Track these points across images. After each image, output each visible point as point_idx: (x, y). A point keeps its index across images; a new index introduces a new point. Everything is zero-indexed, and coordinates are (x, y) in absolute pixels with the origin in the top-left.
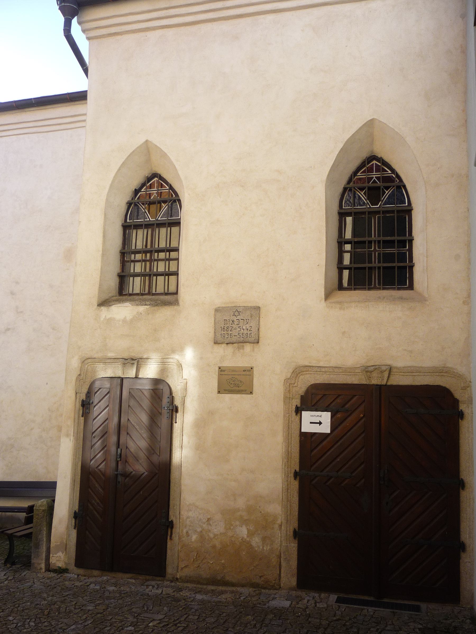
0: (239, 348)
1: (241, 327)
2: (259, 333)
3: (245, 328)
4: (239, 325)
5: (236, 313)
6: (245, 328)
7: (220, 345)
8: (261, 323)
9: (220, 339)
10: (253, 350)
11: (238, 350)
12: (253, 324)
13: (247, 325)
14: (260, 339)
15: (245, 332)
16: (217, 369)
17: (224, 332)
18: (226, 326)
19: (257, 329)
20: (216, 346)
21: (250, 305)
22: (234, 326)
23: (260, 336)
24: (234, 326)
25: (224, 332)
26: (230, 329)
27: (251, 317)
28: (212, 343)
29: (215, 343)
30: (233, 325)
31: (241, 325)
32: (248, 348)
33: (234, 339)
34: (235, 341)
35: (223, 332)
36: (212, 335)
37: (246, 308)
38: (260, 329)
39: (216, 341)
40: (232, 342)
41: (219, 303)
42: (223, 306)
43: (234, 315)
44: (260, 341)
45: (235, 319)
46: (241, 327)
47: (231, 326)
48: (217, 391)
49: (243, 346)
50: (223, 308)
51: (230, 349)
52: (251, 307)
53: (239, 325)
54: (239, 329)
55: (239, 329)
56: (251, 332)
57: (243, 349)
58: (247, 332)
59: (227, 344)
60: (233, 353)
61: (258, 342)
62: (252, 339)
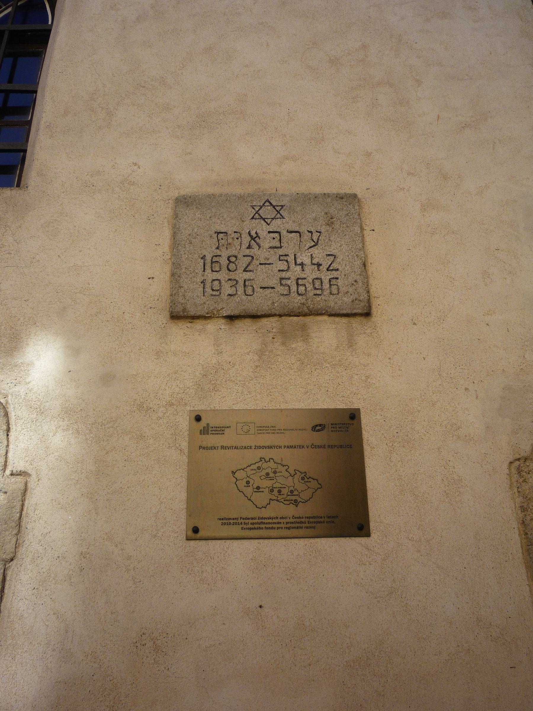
0: (285, 335)
1: (291, 259)
2: (367, 277)
3: (307, 260)
4: (281, 252)
5: (267, 212)
6: (307, 260)
7: (199, 325)
8: (374, 248)
9: (196, 299)
10: (351, 344)
11: (283, 344)
12: (339, 245)
13: (315, 251)
14: (375, 303)
15: (310, 273)
16: (184, 422)
17: (216, 276)
18: (225, 253)
19: (358, 263)
20: (179, 330)
21: (317, 190)
22: (261, 254)
23: (373, 289)
24: (261, 254)
25: (216, 276)
26: (243, 262)
27: (330, 223)
28: (163, 318)
29: (175, 317)
30: (255, 251)
31: (289, 248)
32: (326, 334)
33: (260, 301)
34: (265, 308)
35: (210, 276)
36: (159, 288)
37: (306, 199)
38: (371, 269)
39: (179, 309)
40: (252, 307)
41: (191, 180)
42: (210, 190)
43: (257, 216)
44: (374, 311)
45: (262, 229)
46: (291, 259)
47: (247, 252)
48: (180, 524)
49: (304, 327)
50: (211, 197)
51: (245, 339)
52: (325, 195)
53: (281, 252)
54: (283, 266)
55: (283, 266)
56: (335, 274)
57: (306, 338)
58: (317, 274)
59: (231, 318)
60: (261, 353)
61: (367, 314)
62: (343, 302)
